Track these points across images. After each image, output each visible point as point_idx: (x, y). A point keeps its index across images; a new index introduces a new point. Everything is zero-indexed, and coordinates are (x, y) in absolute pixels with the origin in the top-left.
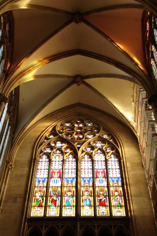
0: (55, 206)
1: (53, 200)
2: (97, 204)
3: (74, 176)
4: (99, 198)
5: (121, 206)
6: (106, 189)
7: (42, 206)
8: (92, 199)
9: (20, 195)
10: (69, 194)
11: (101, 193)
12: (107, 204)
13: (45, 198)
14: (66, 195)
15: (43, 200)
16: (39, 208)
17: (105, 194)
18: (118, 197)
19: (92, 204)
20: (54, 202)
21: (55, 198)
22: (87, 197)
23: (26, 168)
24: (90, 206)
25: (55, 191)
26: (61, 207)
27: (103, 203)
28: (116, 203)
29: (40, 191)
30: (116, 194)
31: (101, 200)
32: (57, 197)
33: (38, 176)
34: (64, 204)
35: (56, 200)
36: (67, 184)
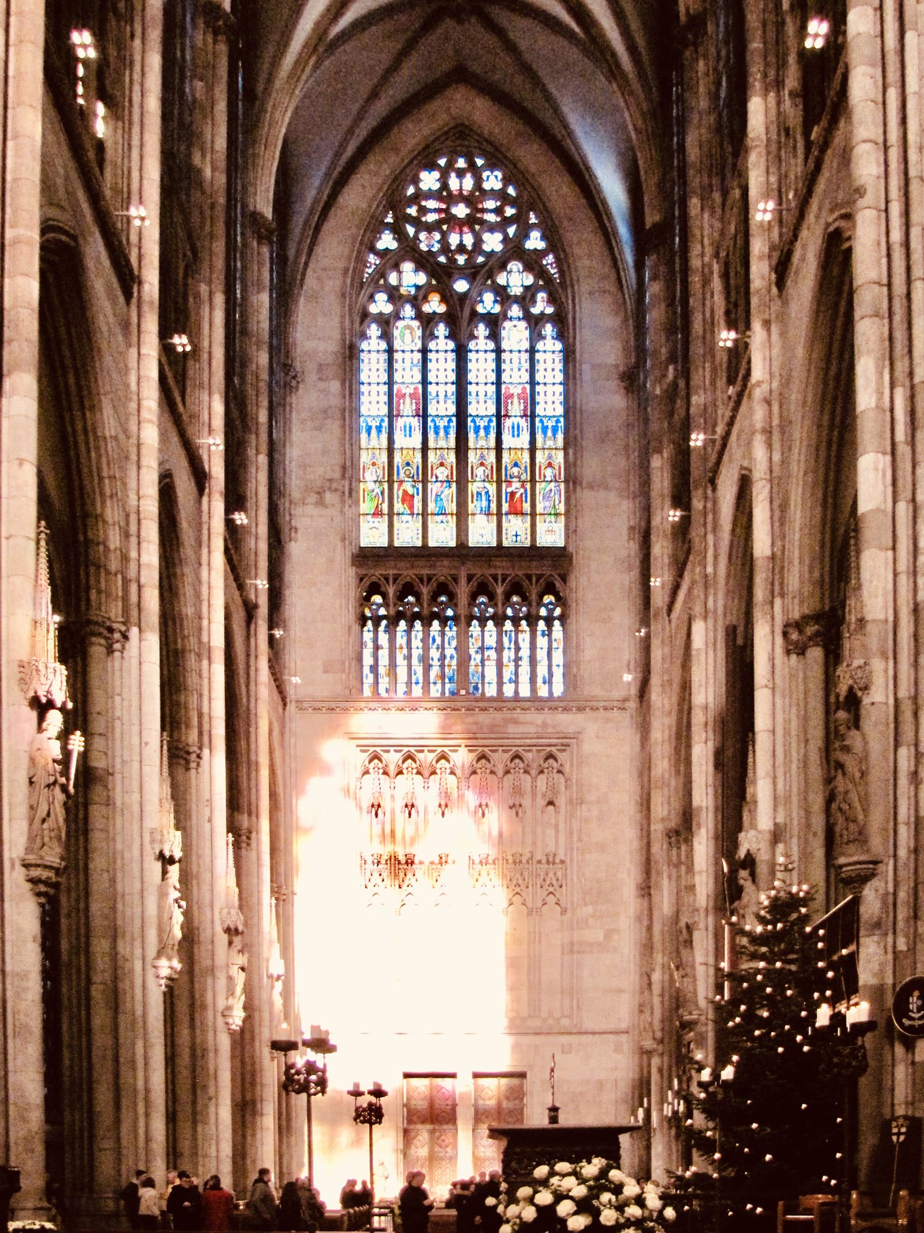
0: (412, 514)
1: (405, 492)
2: (505, 507)
3: (452, 409)
4: (509, 490)
5: (557, 514)
6: (526, 457)
7: (382, 515)
8: (492, 489)
9: (330, 480)
10: (442, 473)
11: (515, 470)
12: (527, 507)
13: (386, 485)
14: (434, 479)
15: (383, 493)
16: (376, 520)
17: (523, 477)
18: (553, 484)
19: (494, 506)
20: (408, 498)
21: (411, 491)
22: (481, 485)
23: (333, 382)
24: (488, 514)
25: (408, 464)
26: (424, 514)
27: (518, 505)
28: (547, 504)
29: (374, 464)
30: (549, 473)
31: (513, 494)
32: (414, 486)
33: (364, 410)
34: (432, 507)
35: (413, 496)
36: (436, 440)
